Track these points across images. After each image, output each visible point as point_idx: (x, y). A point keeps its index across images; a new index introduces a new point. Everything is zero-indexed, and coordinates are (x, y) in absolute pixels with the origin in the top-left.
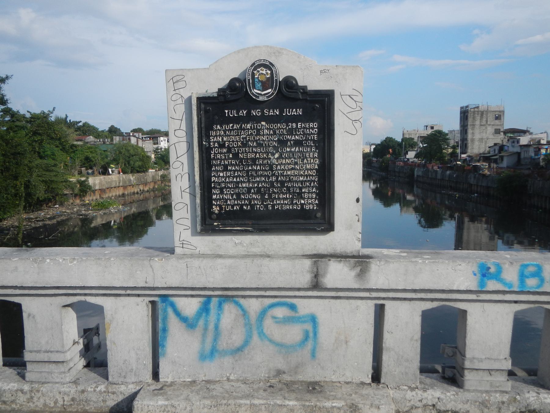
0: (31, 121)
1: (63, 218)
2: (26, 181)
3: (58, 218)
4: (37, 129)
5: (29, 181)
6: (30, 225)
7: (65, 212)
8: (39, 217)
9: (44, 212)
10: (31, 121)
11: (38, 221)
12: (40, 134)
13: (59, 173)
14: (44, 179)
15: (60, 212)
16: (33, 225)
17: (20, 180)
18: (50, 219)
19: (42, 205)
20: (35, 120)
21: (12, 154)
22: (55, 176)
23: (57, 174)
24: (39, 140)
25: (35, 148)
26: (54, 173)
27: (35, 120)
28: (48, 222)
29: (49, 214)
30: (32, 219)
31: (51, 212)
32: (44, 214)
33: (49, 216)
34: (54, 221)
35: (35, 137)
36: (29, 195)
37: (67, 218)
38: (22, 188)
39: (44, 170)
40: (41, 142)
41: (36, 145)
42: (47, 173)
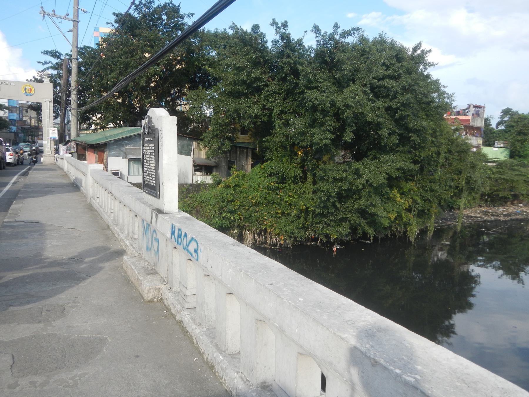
0: (518, 121)
1: (519, 217)
2: (468, 176)
3: (514, 216)
4: (523, 129)
5: (471, 177)
6: (483, 218)
7: (526, 212)
8: (496, 213)
9: (505, 208)
10: (518, 121)
11: (492, 215)
12: (525, 134)
13: (521, 172)
14: (505, 177)
15: (520, 211)
16: (486, 218)
17: (462, 175)
18: (505, 216)
19: (506, 202)
20: (522, 120)
21: (458, 152)
22: (517, 175)
23: (520, 173)
24: (522, 140)
25: (516, 147)
26: (517, 173)
27: (522, 120)
28: (502, 218)
29: (507, 211)
30: (489, 212)
31: (511, 209)
32: (503, 211)
33: (505, 213)
34: (508, 219)
35: (519, 137)
36: (471, 190)
37: (523, 217)
38: (464, 183)
39: (509, 169)
40: (524, 142)
41: (518, 144)
42: (511, 172)
